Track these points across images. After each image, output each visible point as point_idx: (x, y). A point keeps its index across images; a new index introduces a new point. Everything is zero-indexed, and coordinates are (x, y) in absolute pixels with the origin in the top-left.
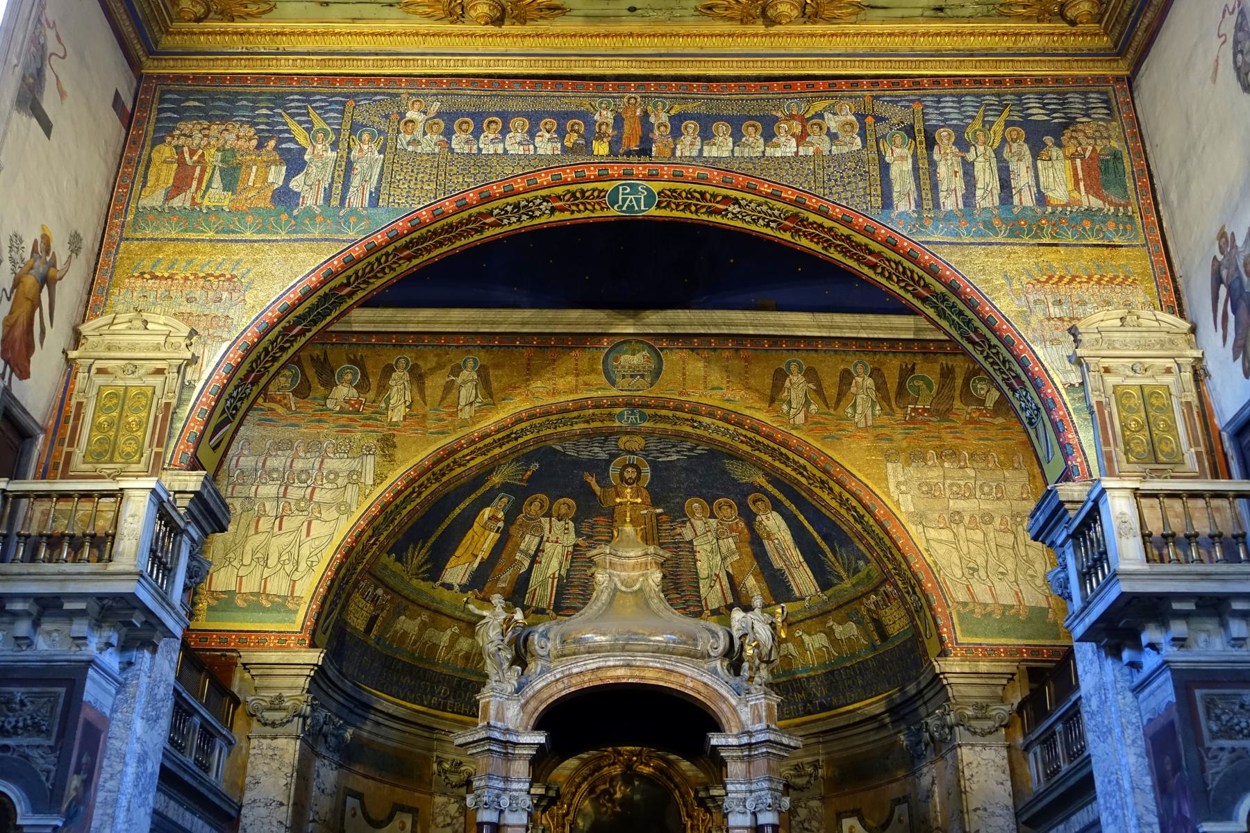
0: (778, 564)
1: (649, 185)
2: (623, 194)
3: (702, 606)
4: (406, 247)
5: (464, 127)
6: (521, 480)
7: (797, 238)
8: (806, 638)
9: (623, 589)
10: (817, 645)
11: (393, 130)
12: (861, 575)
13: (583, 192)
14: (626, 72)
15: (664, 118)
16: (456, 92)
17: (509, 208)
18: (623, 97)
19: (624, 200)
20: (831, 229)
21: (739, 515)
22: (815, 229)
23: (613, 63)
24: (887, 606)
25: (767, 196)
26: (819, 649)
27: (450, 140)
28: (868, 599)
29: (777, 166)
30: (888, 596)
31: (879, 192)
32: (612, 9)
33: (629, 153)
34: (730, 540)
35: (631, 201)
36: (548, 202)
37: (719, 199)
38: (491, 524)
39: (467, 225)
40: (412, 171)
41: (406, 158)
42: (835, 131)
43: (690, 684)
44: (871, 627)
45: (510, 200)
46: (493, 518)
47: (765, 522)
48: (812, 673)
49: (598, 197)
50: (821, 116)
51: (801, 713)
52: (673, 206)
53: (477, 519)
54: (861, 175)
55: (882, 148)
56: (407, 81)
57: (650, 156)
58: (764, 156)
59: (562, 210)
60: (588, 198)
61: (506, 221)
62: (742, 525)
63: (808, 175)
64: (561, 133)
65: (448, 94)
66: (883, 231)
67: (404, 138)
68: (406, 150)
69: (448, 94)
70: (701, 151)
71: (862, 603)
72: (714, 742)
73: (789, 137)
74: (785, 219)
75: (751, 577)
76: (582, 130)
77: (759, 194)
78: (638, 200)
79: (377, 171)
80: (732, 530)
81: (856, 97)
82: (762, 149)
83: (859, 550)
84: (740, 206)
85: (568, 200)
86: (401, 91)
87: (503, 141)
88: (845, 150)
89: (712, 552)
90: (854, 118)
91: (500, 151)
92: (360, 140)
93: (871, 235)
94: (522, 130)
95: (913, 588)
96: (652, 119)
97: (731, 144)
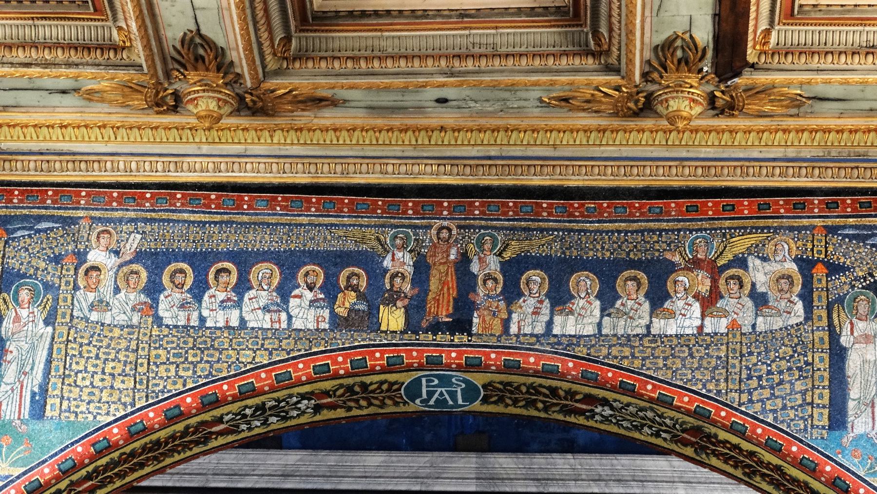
1: (468, 376)
2: (427, 386)
4: (89, 477)
5: (179, 278)
7: (704, 456)
11: (67, 283)
13: (364, 386)
14: (436, 182)
15: (493, 264)
16: (165, 215)
17: (248, 412)
18: (429, 227)
19: (430, 394)
20: (752, 454)
22: (729, 449)
23: (416, 169)
25: (651, 400)
27: (156, 301)
29: (668, 350)
31: (826, 400)
32: (410, 100)
33: (436, 327)
35: (441, 394)
36: (309, 399)
37: (578, 397)
39: (181, 437)
40: (97, 357)
41: (87, 334)
42: (761, 289)
45: (249, 402)
49: (387, 391)
50: (741, 262)
52: (509, 401)
54: (800, 369)
55: (836, 322)
56: (88, 195)
57: (470, 334)
58: (649, 332)
59: (332, 407)
60: (373, 391)
61: (244, 427)
63: (716, 368)
64: (331, 291)
65: (152, 220)
66: (828, 469)
67: (85, 297)
68: (87, 320)
69: (152, 220)
70: (550, 324)
73: (690, 300)
74: (684, 431)
76: (364, 284)
77: (640, 397)
78: (453, 395)
79: (42, 356)
81: (799, 229)
82: (645, 321)
84: (612, 408)
85: (342, 395)
86: (81, 213)
87: (239, 304)
88: (778, 323)
90: (794, 267)
91: (234, 323)
92: (16, 300)
93: (813, 471)
94: (269, 285)
96: (475, 268)
97: (597, 313)
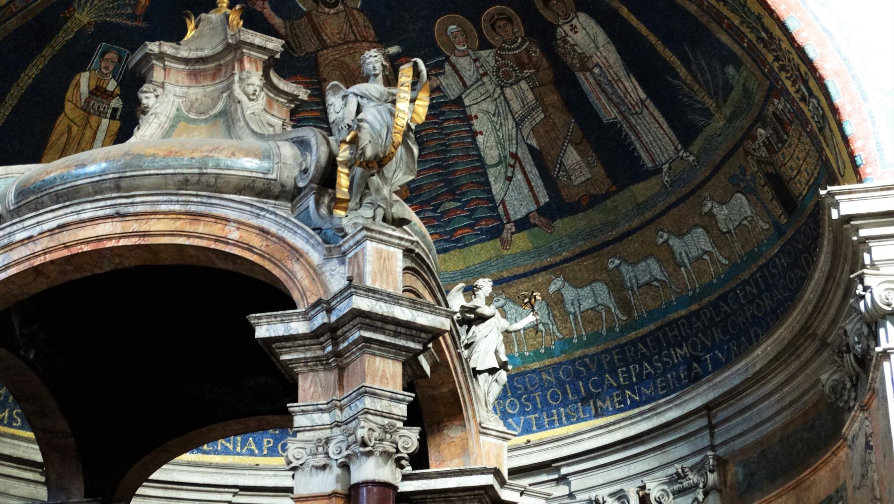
0: (609, 113)
3: (499, 217)
6: (133, 17)
8: (675, 242)
9: (192, 116)
10: (694, 253)
12: (736, 95)
21: (528, 33)
24: (784, 142)
26: (699, 258)
28: (754, 138)
30: (780, 121)
34: (523, 84)
38: (95, 103)
43: (235, 235)
44: (767, 193)
46: (98, 92)
47: (573, 38)
48: (694, 307)
51: (685, 381)
53: (69, 95)
62: (536, 53)
71: (747, 153)
72: (261, 332)
75: (571, 148)
80: (522, 66)
83: (723, 45)
89: (497, 114)
95: (806, 83)
